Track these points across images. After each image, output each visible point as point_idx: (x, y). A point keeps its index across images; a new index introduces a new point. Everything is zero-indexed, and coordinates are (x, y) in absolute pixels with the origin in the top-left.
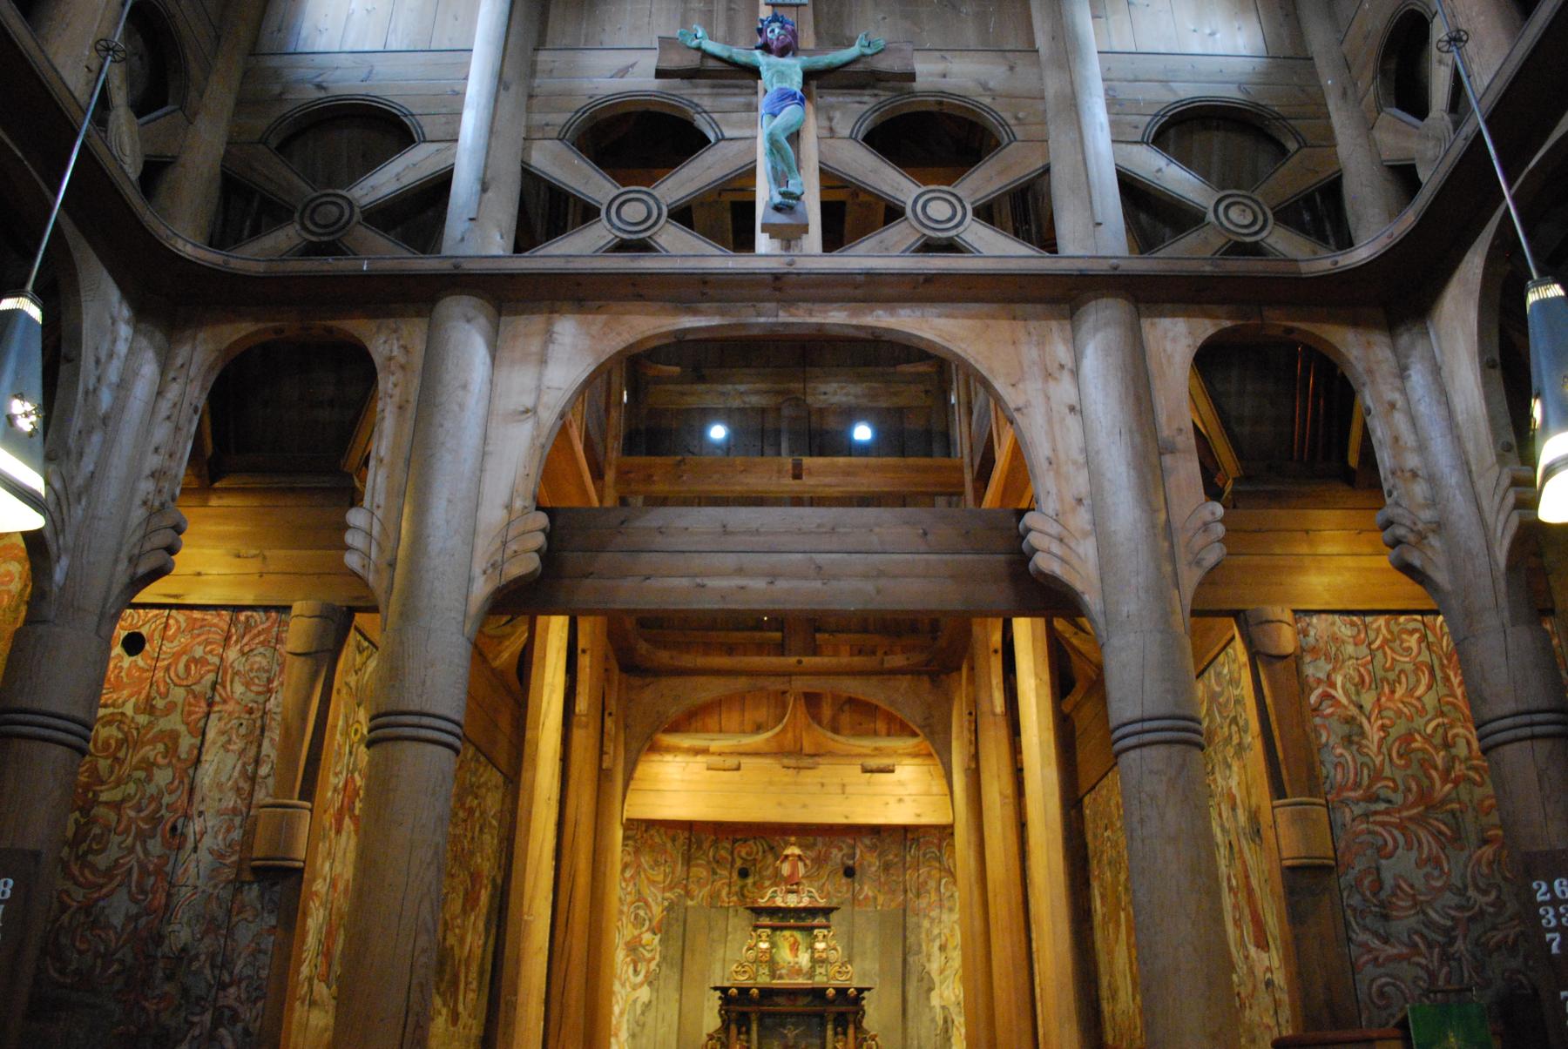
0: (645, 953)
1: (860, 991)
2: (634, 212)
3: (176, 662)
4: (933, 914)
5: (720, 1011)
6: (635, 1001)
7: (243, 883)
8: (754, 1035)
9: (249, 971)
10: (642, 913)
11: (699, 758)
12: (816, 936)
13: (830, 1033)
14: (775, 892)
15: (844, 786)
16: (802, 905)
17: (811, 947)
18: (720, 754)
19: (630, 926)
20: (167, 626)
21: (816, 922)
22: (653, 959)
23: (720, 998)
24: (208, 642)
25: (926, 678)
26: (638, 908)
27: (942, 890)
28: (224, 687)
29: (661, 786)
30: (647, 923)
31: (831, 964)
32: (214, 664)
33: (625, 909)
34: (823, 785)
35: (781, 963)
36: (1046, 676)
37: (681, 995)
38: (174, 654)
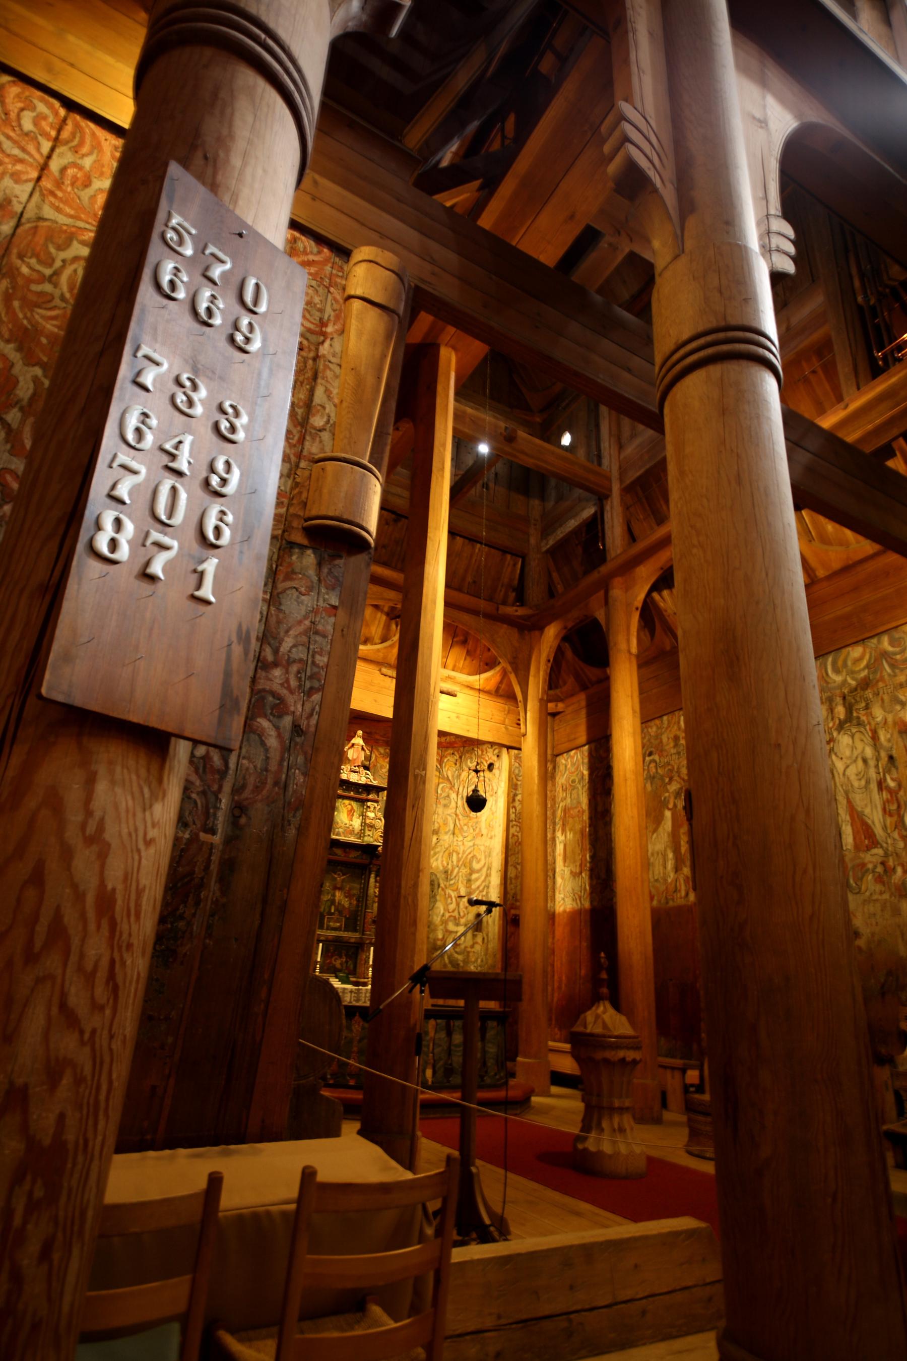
7: (292, 545)
9: (300, 653)
13: (372, 880)
16: (360, 782)
17: (363, 816)
25: (516, 630)
27: (439, 792)
35: (340, 824)
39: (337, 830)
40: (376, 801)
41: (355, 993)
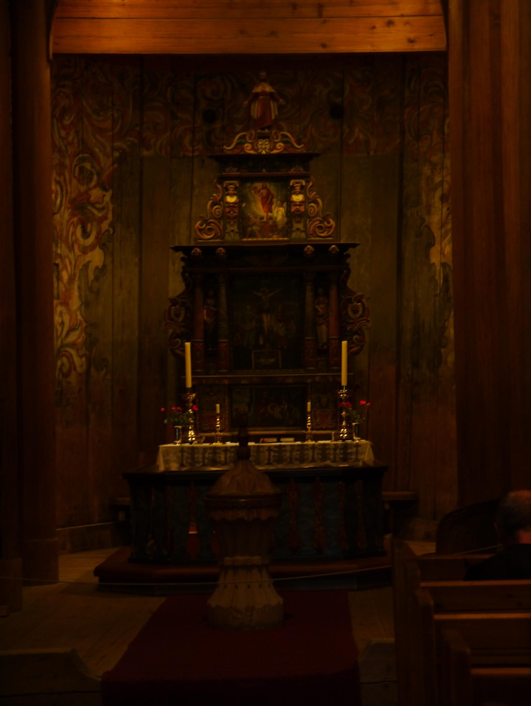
0: (95, 212)
1: (344, 247)
4: (435, 159)
5: (183, 274)
6: (86, 266)
8: (223, 300)
10: (88, 166)
12: (293, 187)
13: (309, 294)
14: (243, 137)
15: (320, 7)
16: (275, 151)
17: (287, 201)
19: (74, 182)
21: (292, 171)
22: (105, 218)
23: (183, 259)
26: (83, 160)
27: (446, 130)
30: (95, 177)
31: (311, 218)
33: (67, 162)
34: (295, 6)
37: (141, 260)
39: (249, 229)
40: (305, 177)
41: (275, 451)
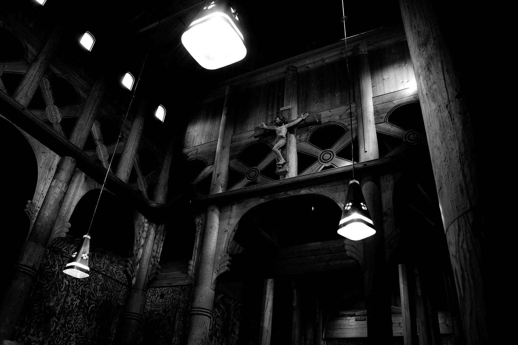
2: (253, 174)
3: (170, 300)
11: (353, 318)
15: (400, 323)
18: (359, 316)
20: (168, 291)
24: (176, 294)
28: (180, 305)
29: (342, 327)
32: (177, 300)
36: (406, 283)
38: (170, 298)
